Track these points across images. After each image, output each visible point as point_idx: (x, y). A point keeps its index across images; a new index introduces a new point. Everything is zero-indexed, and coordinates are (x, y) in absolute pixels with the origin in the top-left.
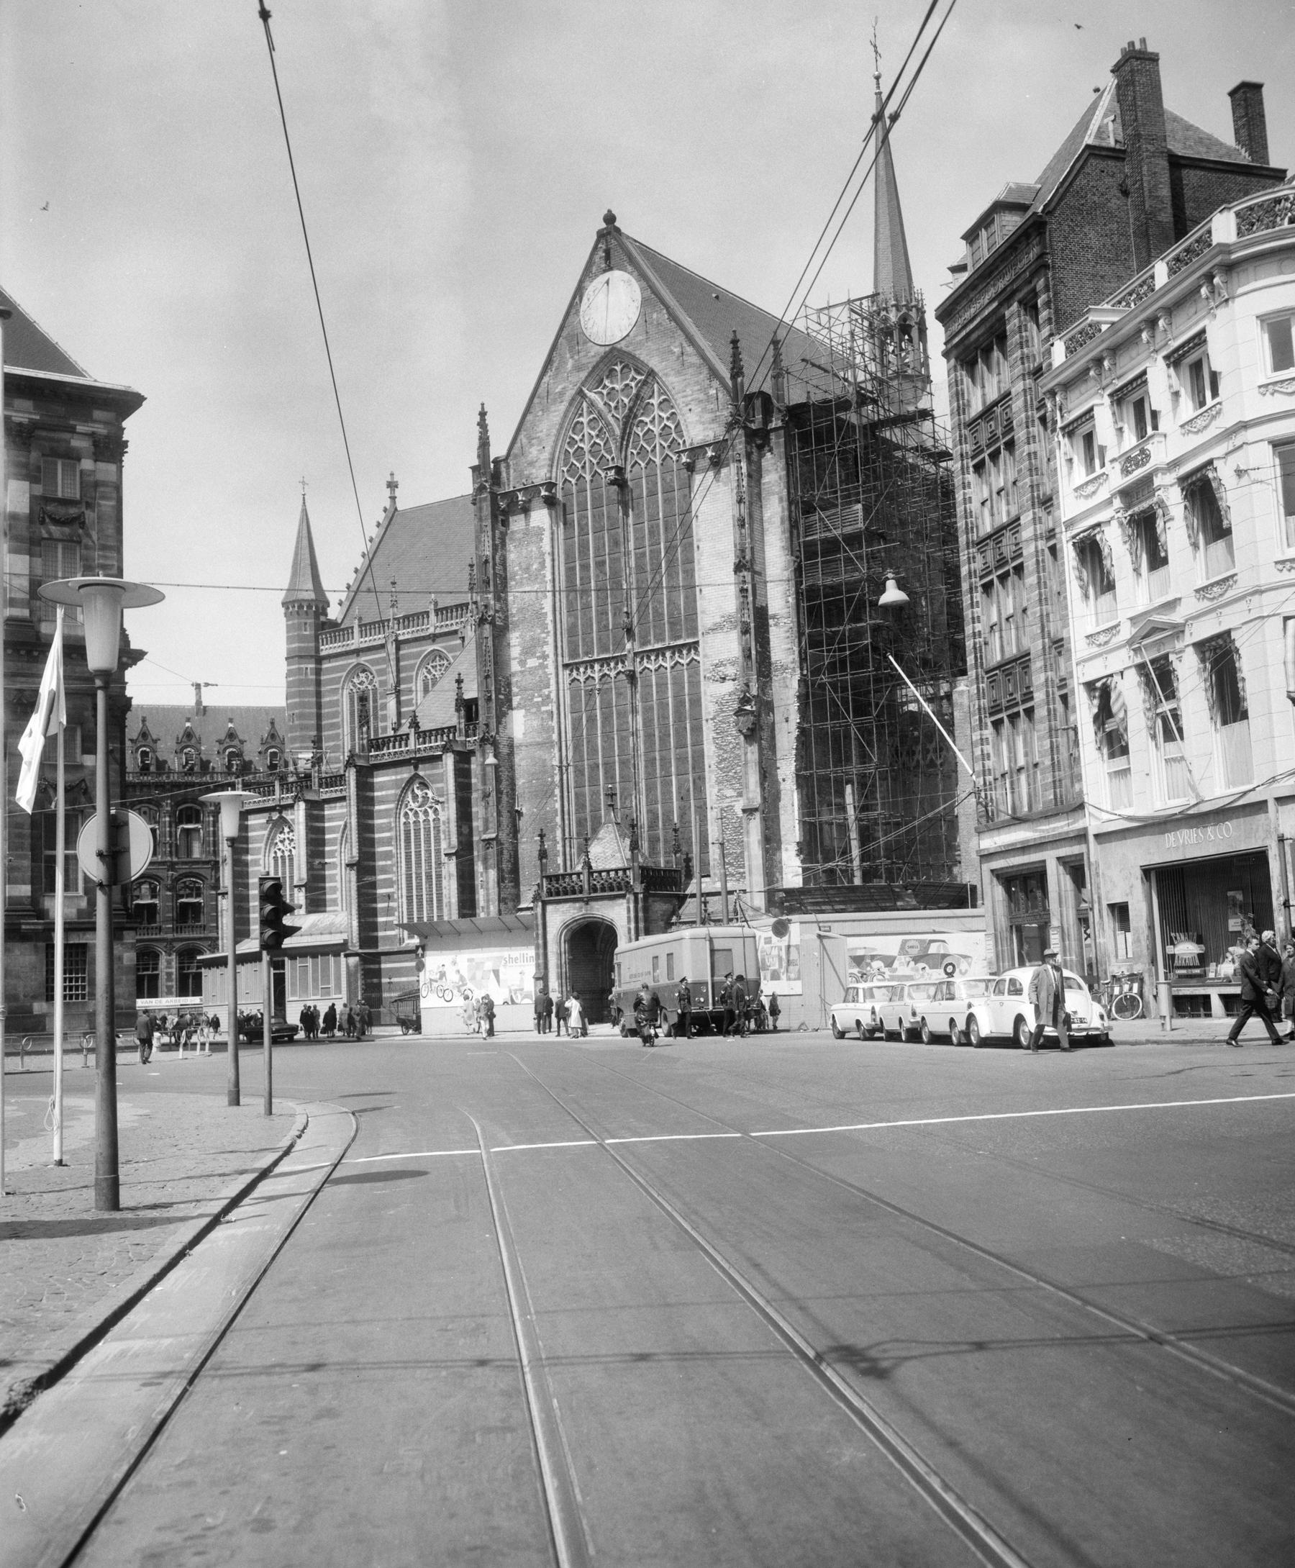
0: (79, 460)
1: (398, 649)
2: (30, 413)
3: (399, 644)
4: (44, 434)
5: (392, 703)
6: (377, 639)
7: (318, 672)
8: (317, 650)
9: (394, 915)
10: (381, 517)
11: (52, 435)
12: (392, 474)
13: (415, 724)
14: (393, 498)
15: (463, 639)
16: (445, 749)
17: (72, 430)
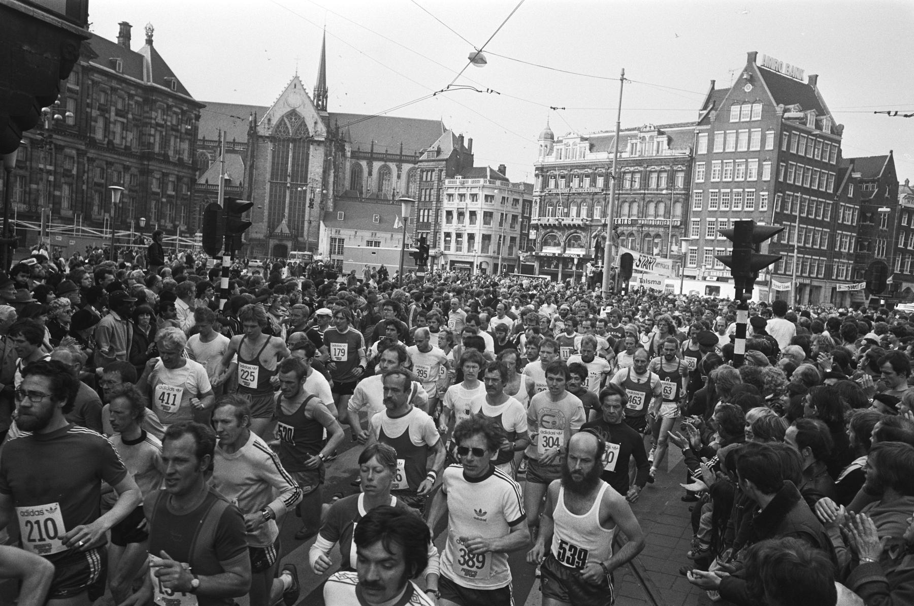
13: (207, 181)
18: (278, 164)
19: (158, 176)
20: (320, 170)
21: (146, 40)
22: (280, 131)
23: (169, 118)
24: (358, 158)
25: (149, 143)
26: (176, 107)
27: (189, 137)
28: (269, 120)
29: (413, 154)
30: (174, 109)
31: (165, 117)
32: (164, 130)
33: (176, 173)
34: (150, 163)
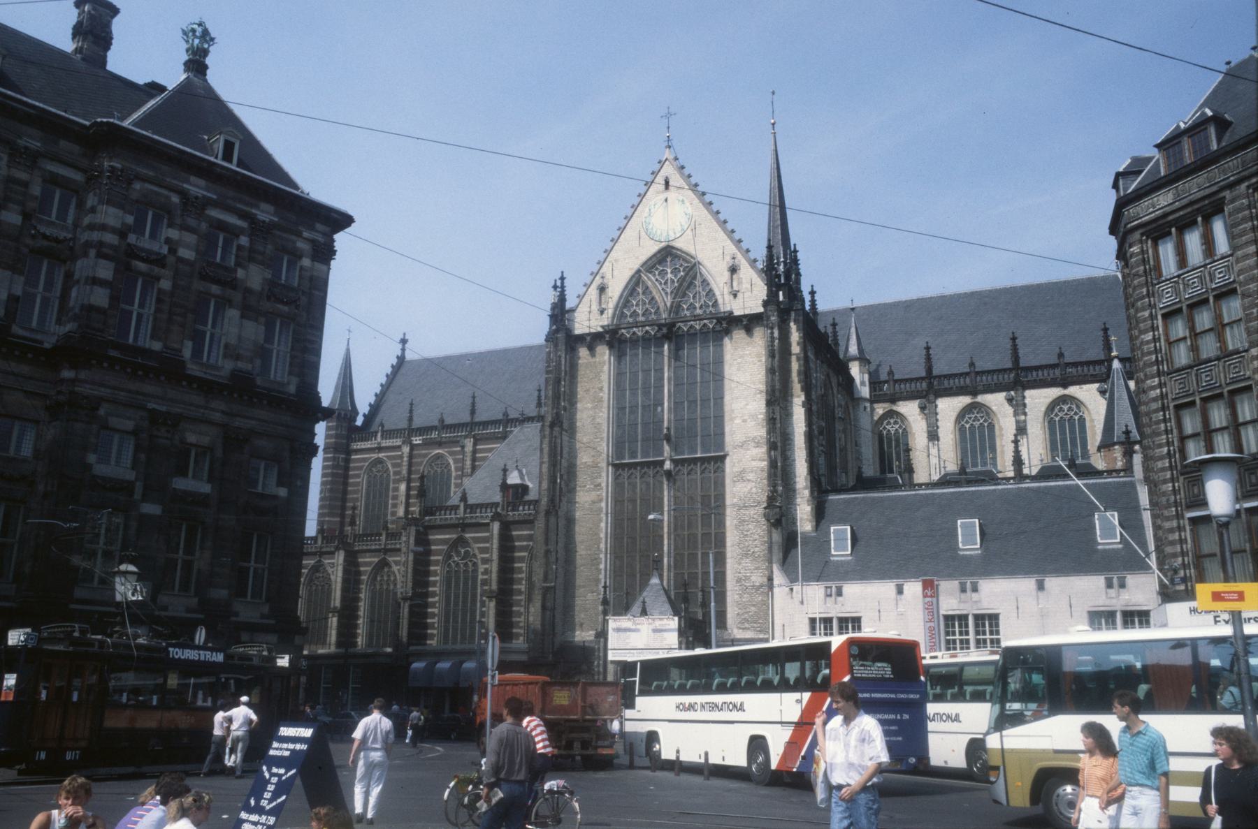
0: (300, 257)
1: (412, 450)
2: (271, 215)
3: (413, 447)
4: (278, 233)
5: (403, 487)
6: (398, 442)
7: (347, 461)
8: (348, 445)
9: (433, 639)
10: (394, 361)
11: (285, 235)
12: (404, 334)
13: (464, 498)
14: (403, 350)
15: (463, 447)
16: (493, 519)
17: (299, 235)
18: (633, 409)
19: (129, 425)
20: (758, 406)
21: (186, 64)
22: (634, 314)
23: (190, 238)
24: (893, 400)
25: (90, 309)
26: (220, 205)
27: (286, 308)
28: (602, 289)
29: (1054, 360)
30: (214, 213)
31: (174, 234)
32: (166, 272)
33: (217, 417)
34: (83, 375)
